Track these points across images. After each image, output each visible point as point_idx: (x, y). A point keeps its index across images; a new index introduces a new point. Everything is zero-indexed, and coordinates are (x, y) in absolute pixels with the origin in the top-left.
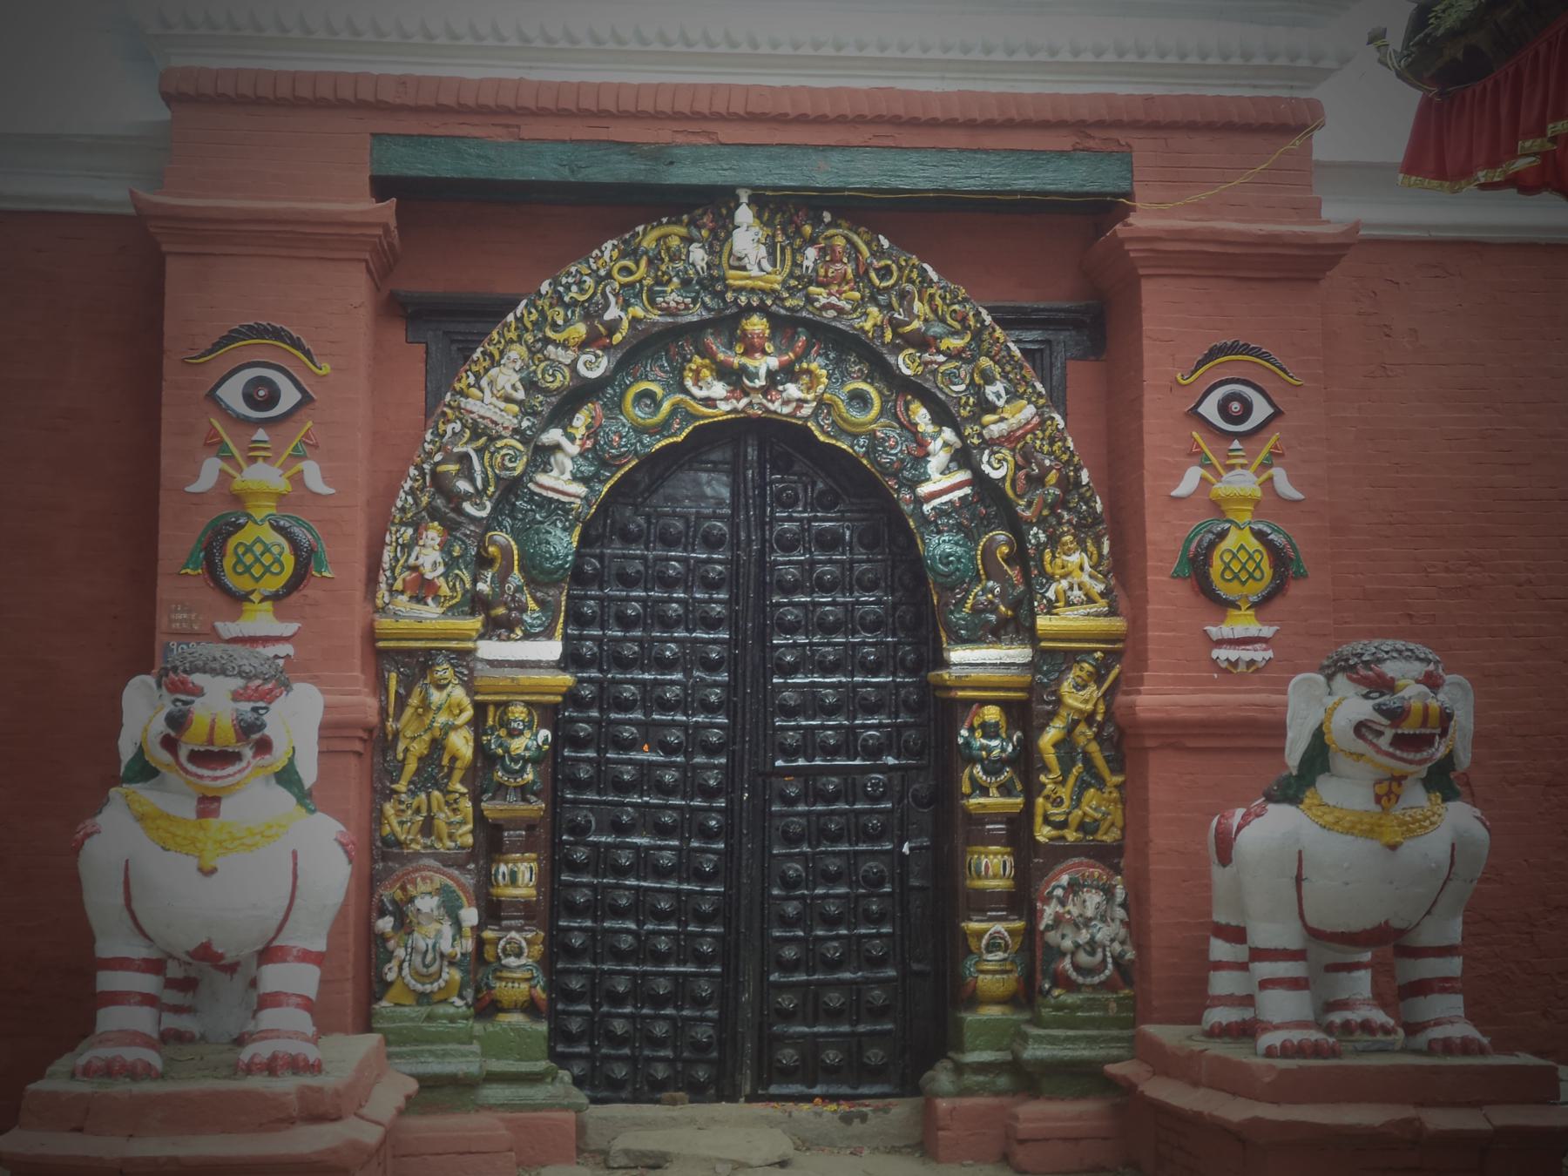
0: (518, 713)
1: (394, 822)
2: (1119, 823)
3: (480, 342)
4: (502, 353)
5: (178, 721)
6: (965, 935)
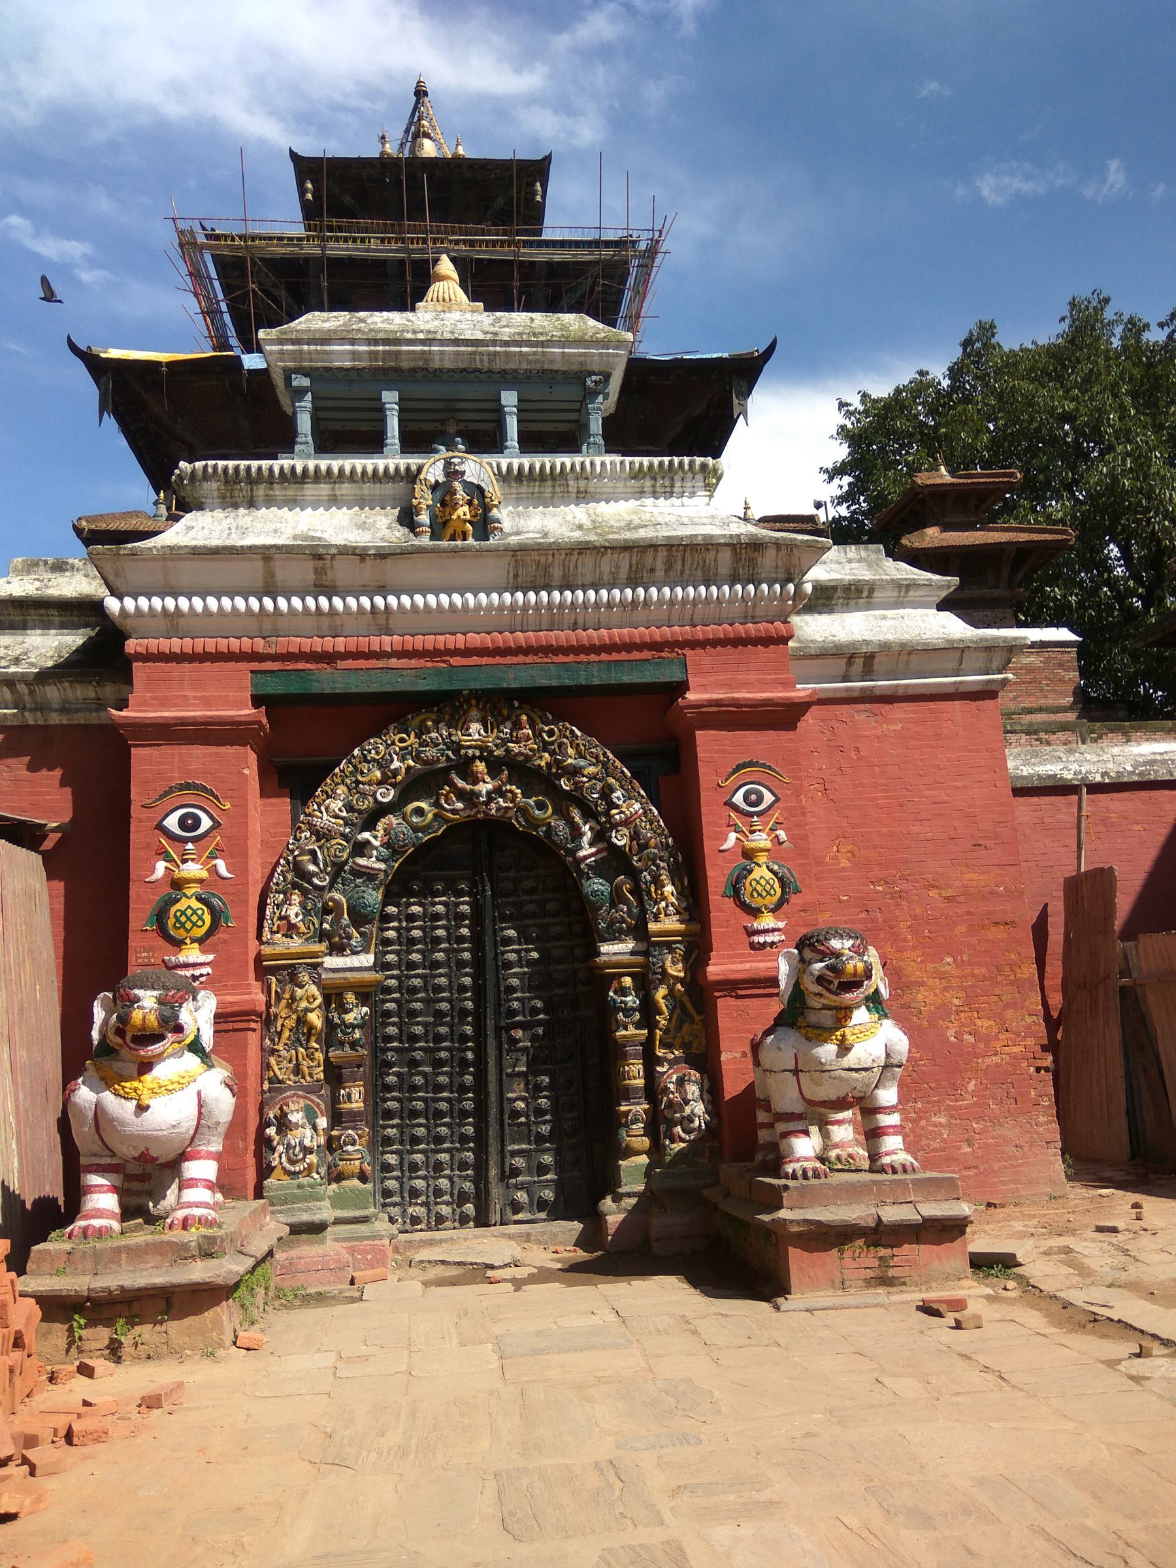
0: (350, 997)
1: (276, 1068)
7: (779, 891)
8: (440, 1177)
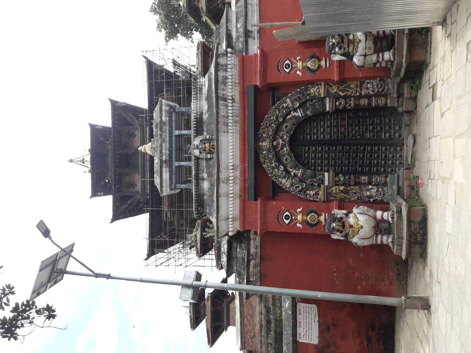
0: (336, 179)
1: (354, 198)
2: (356, 81)
3: (278, 185)
5: (338, 230)
6: (375, 106)
7: (314, 59)
8: (389, 156)
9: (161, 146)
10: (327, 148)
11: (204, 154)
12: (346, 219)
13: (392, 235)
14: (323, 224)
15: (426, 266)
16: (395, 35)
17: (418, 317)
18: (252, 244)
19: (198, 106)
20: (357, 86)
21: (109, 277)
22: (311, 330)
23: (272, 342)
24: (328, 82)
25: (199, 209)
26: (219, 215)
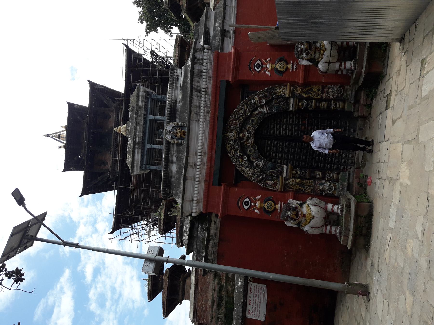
0: (294, 172)
1: (308, 191)
4: (243, 170)
5: (292, 219)
7: (283, 62)
9: (136, 128)
10: (287, 144)
11: (175, 139)
12: (300, 209)
13: (340, 227)
14: (278, 212)
15: (368, 257)
16: (357, 47)
17: (357, 302)
18: (213, 225)
19: (173, 94)
20: (319, 90)
21: (77, 246)
22: (260, 308)
23: (222, 317)
24: (294, 84)
25: (166, 189)
26: (185, 197)
